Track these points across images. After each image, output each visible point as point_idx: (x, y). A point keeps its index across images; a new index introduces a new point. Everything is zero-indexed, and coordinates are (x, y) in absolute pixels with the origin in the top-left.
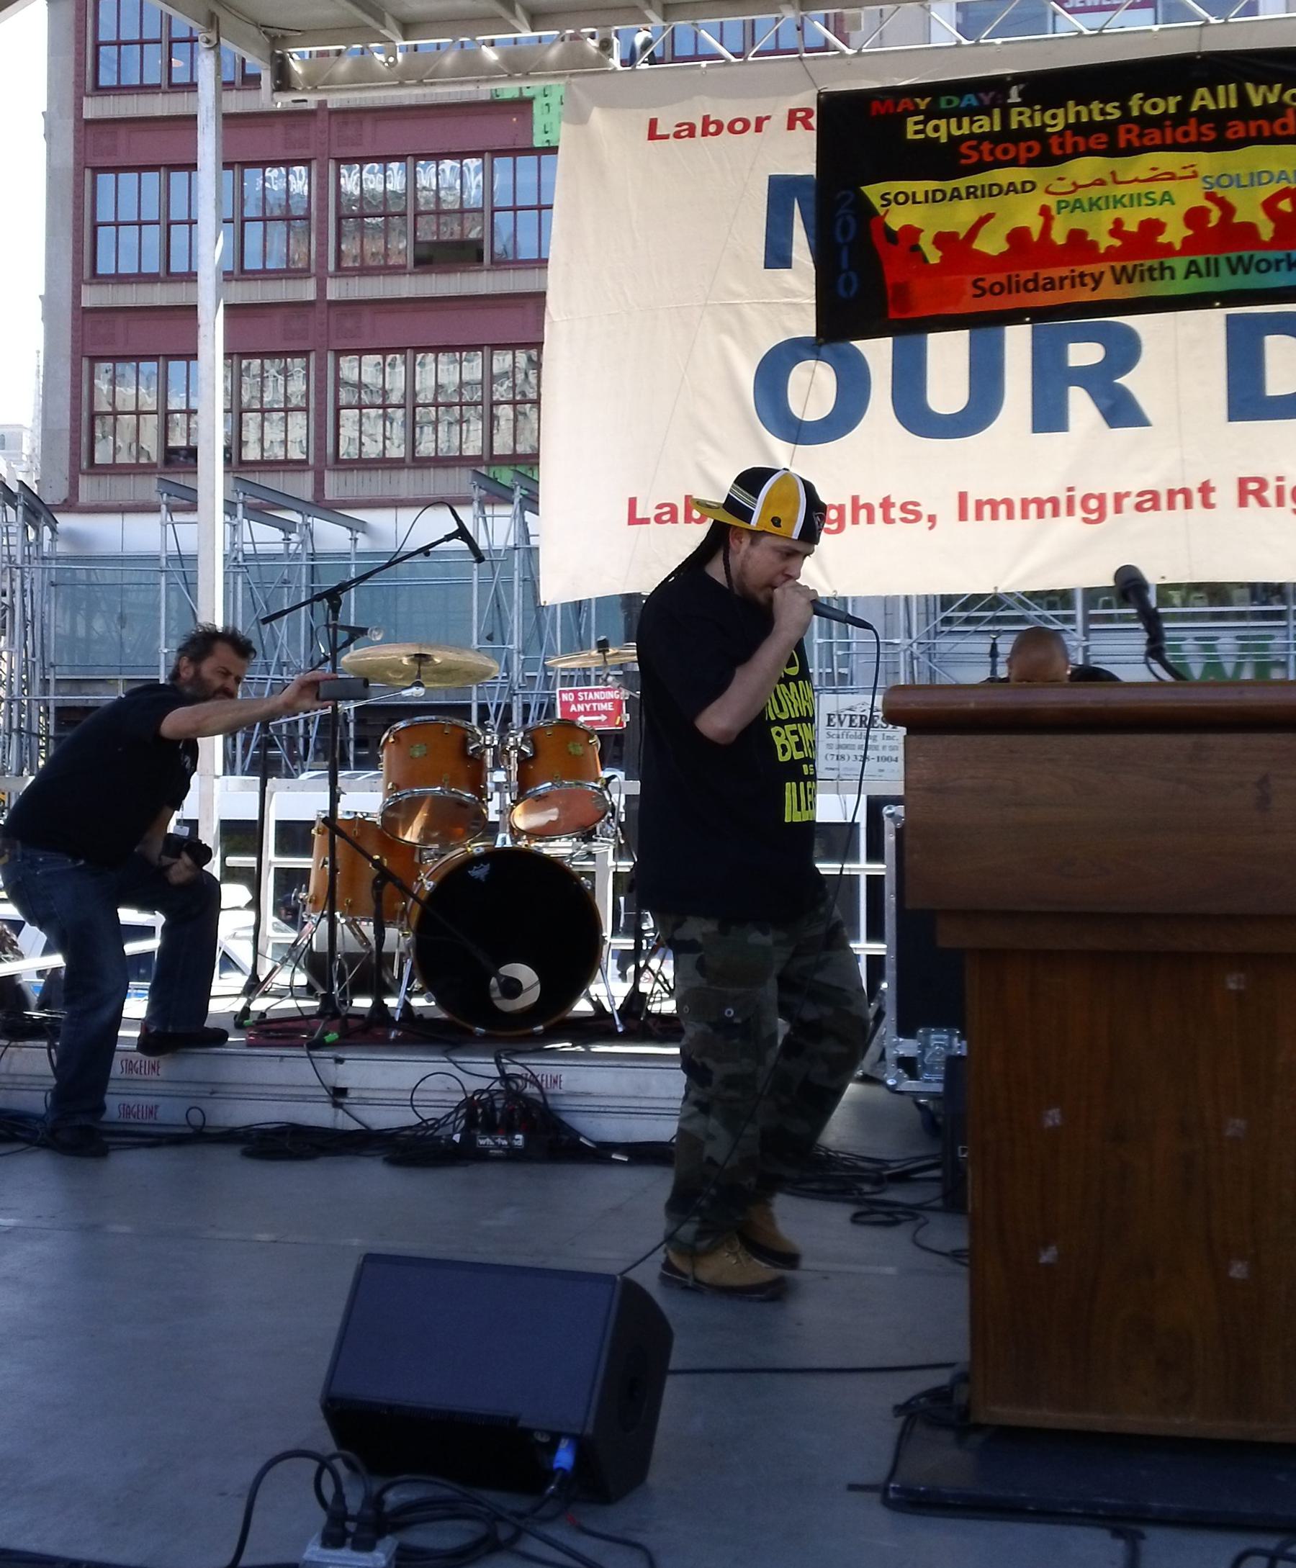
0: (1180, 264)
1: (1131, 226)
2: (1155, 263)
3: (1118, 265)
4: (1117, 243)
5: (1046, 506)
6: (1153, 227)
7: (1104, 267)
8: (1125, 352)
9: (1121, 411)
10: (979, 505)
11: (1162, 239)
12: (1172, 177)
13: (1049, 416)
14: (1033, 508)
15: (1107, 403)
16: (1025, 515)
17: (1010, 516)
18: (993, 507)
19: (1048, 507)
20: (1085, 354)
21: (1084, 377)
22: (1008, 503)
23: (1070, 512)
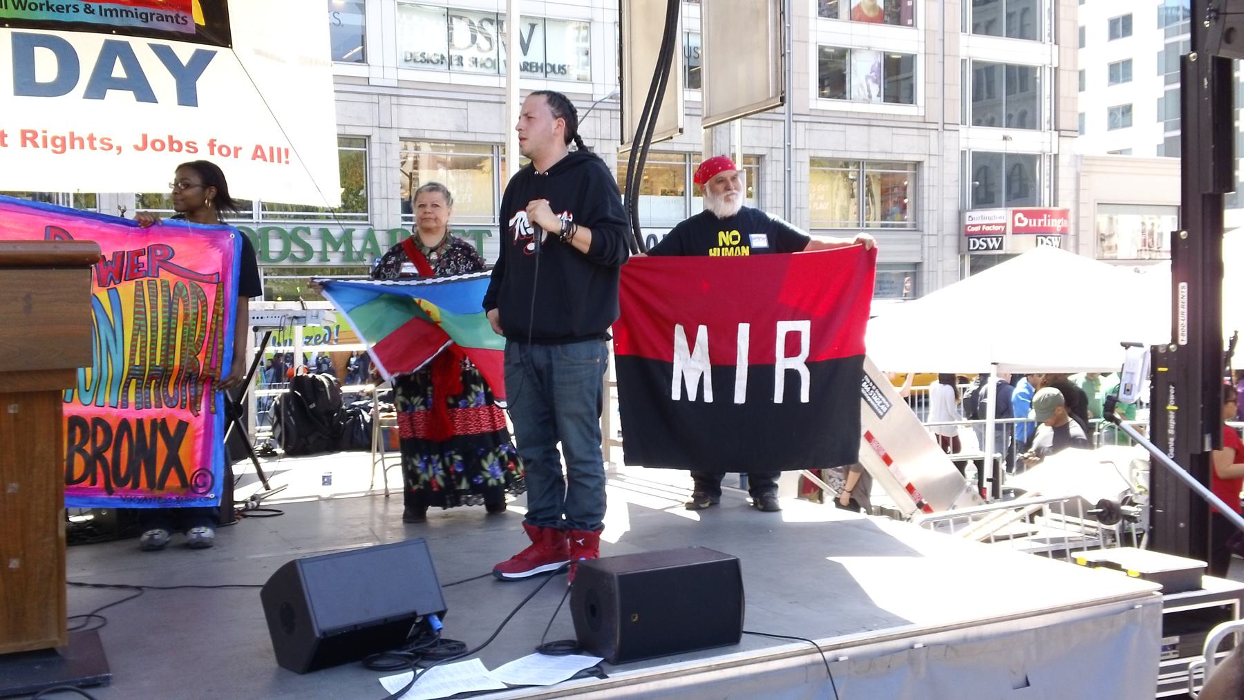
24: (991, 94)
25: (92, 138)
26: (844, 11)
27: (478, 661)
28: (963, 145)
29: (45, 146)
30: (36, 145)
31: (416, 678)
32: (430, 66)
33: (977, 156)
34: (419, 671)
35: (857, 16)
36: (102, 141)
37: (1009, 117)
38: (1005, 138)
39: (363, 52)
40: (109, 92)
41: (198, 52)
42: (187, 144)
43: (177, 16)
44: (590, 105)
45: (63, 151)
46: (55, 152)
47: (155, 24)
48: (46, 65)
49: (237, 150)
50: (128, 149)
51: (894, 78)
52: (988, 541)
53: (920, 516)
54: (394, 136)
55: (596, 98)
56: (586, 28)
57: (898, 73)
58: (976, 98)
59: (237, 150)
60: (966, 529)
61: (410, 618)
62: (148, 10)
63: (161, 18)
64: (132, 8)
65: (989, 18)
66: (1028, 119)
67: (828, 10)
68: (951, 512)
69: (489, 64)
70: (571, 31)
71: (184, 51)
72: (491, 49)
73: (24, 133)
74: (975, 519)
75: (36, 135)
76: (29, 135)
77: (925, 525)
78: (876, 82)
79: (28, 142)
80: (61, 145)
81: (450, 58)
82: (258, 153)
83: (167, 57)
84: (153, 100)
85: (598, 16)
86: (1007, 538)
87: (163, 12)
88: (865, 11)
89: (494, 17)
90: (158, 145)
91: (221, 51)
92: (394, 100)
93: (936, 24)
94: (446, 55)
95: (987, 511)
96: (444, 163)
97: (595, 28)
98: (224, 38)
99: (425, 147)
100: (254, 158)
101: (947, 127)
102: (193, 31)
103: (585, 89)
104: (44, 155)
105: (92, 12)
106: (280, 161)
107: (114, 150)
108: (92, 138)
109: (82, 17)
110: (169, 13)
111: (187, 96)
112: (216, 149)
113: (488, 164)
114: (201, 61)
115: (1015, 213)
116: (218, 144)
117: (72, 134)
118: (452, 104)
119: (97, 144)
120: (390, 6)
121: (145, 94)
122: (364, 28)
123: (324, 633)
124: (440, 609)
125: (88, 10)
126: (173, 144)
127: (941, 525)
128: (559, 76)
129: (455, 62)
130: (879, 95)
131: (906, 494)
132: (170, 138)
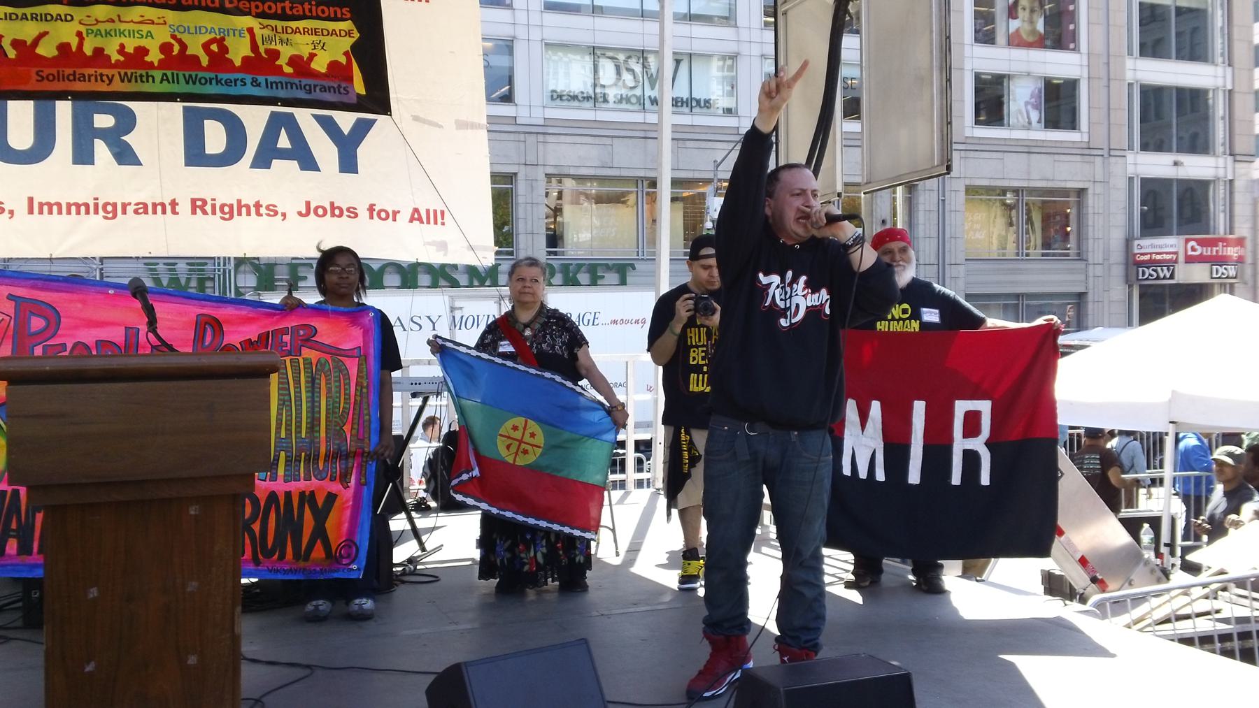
0: (158, 74)
1: (130, 49)
2: (144, 73)
3: (122, 72)
4: (122, 58)
6: (142, 51)
7: (115, 72)
8: (127, 122)
9: (125, 156)
10: (41, 205)
11: (147, 59)
12: (153, 23)
13: (83, 155)
14: (73, 208)
15: (117, 150)
16: (69, 213)
17: (60, 212)
18: (50, 207)
19: (83, 208)
20: (103, 121)
21: (104, 134)
22: (59, 205)
23: (96, 212)
25: (258, 205)
29: (214, 213)
30: (205, 213)
36: (268, 208)
41: (359, 121)
42: (348, 210)
45: (231, 217)
46: (223, 218)
47: (318, 95)
48: (215, 138)
49: (395, 213)
50: (292, 216)
59: (395, 213)
63: (324, 89)
64: (296, 81)
71: (346, 120)
73: (194, 201)
76: (199, 203)
79: (198, 210)
80: (229, 212)
82: (416, 216)
83: (330, 127)
87: (326, 83)
90: (320, 211)
91: (381, 118)
98: (383, 106)
100: (411, 221)
102: (354, 100)
105: (259, 85)
106: (436, 223)
107: (279, 217)
108: (258, 205)
109: (250, 90)
110: (332, 84)
111: (348, 164)
112: (375, 214)
114: (362, 129)
116: (377, 208)
117: (239, 202)
119: (263, 210)
121: (308, 162)
125: (255, 83)
132: (332, 204)
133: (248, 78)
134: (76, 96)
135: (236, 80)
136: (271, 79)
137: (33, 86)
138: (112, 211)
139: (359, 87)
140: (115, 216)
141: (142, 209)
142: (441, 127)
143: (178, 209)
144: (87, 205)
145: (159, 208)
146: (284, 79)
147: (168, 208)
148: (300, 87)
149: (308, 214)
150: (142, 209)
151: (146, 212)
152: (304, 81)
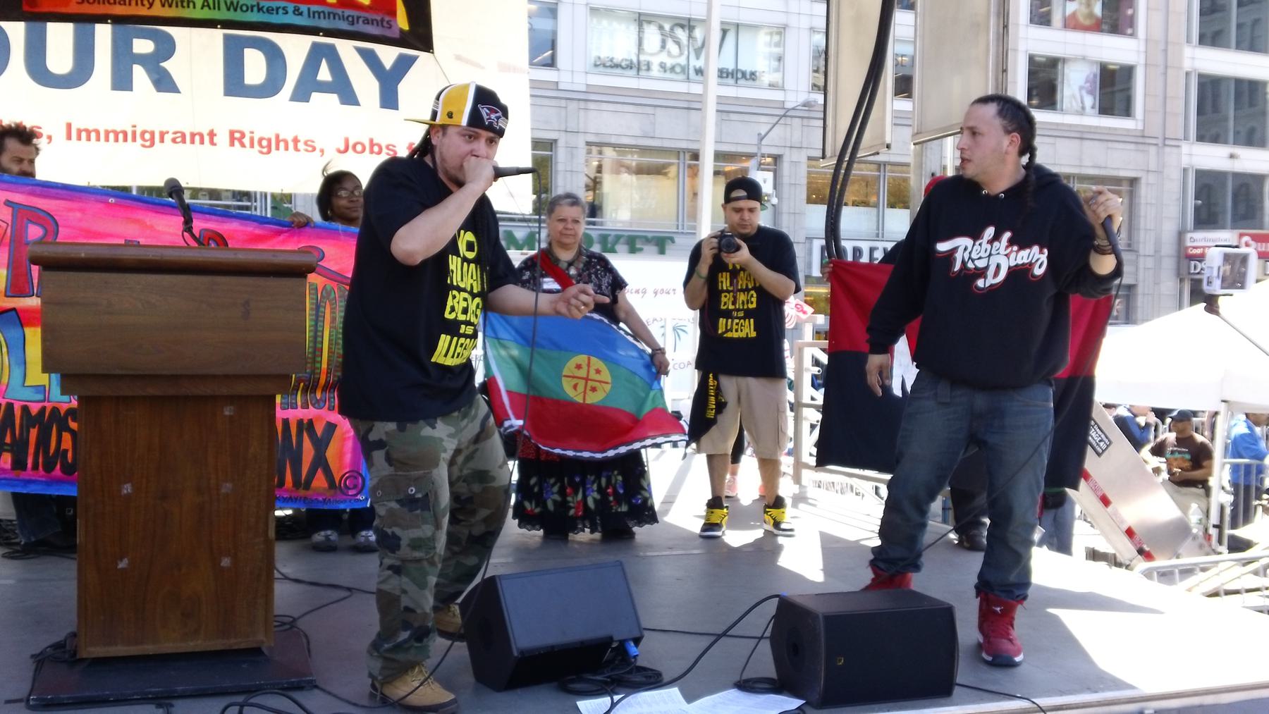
5: (120, 135)
8: (167, 48)
9: (164, 83)
10: (79, 132)
13: (122, 81)
14: (112, 136)
15: (156, 76)
17: (98, 139)
19: (121, 136)
20: (143, 46)
21: (142, 60)
23: (134, 139)
24: (1216, 109)
25: (296, 141)
26: (1057, 18)
27: (674, 692)
28: (1185, 161)
29: (252, 146)
30: (243, 145)
31: (613, 705)
32: (619, 71)
33: (1201, 174)
34: (616, 698)
35: (1072, 24)
36: (306, 143)
37: (1237, 133)
38: (1232, 156)
39: (553, 57)
40: (314, 94)
43: (382, 20)
44: (782, 112)
45: (269, 152)
47: (361, 27)
48: (255, 66)
51: (1109, 90)
52: (1215, 594)
53: (1143, 565)
54: (581, 141)
55: (788, 105)
56: (779, 33)
57: (1113, 84)
58: (1200, 111)
60: (1191, 581)
61: (605, 643)
62: (355, 13)
63: (366, 21)
64: (339, 11)
65: (1217, 28)
66: (1257, 136)
67: (1041, 17)
68: (1174, 561)
69: (678, 69)
70: (763, 37)
71: (388, 55)
72: (681, 54)
73: (232, 133)
74: (1204, 570)
75: (243, 135)
76: (237, 135)
77: (1148, 574)
78: (1091, 92)
79: (236, 143)
80: (269, 145)
81: (639, 62)
84: (357, 104)
85: (793, 21)
86: (1237, 592)
88: (1081, 19)
89: (685, 23)
90: (359, 148)
91: (423, 56)
92: (582, 105)
93: (1158, 34)
94: (635, 60)
95: (1217, 562)
96: (629, 170)
97: (791, 36)
98: (427, 46)
99: (609, 153)
101: (1167, 142)
102: (397, 35)
103: (777, 96)
104: (251, 155)
105: (301, 14)
107: (317, 152)
109: (291, 19)
111: (389, 99)
113: (673, 171)
114: (404, 65)
115: (1241, 235)
117: (277, 136)
118: (640, 109)
119: (301, 146)
120: (582, 12)
121: (348, 96)
122: (555, 33)
123: (522, 652)
124: (637, 634)
125: (297, 12)
126: (373, 147)
127: (1165, 576)
128: (750, 83)
129: (644, 68)
130: (1093, 107)
131: (1126, 539)
132: (371, 141)
133: (291, 7)
134: (117, 20)
135: (278, 9)
136: (314, 8)
137: (73, 8)
138: (150, 139)
139: (402, 22)
140: (152, 144)
141: (180, 138)
142: (483, 68)
143: (216, 140)
144: (125, 134)
145: (197, 138)
146: (327, 9)
147: (207, 139)
148: (343, 18)
149: (346, 150)
150: (180, 138)
151: (184, 141)
152: (348, 12)
